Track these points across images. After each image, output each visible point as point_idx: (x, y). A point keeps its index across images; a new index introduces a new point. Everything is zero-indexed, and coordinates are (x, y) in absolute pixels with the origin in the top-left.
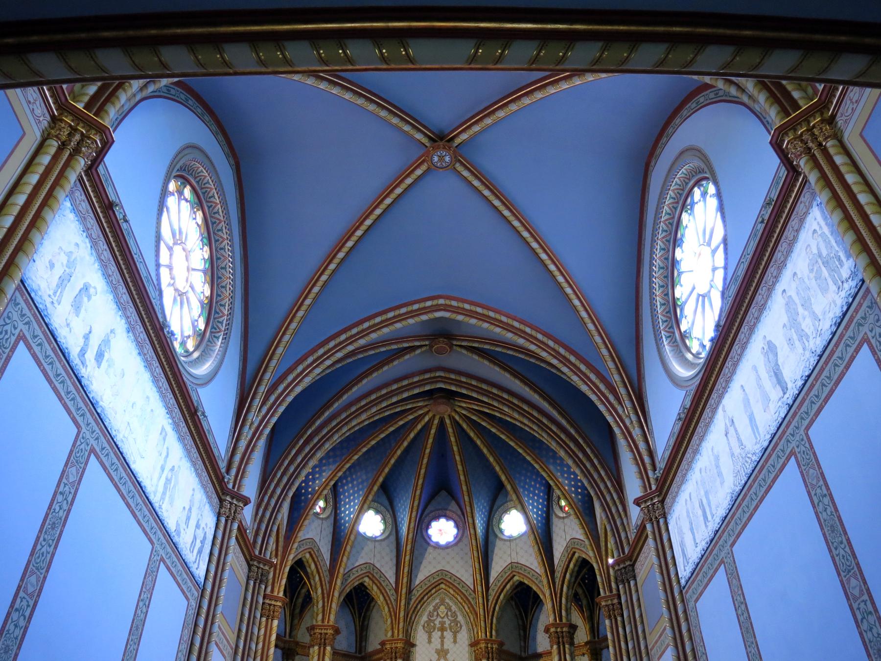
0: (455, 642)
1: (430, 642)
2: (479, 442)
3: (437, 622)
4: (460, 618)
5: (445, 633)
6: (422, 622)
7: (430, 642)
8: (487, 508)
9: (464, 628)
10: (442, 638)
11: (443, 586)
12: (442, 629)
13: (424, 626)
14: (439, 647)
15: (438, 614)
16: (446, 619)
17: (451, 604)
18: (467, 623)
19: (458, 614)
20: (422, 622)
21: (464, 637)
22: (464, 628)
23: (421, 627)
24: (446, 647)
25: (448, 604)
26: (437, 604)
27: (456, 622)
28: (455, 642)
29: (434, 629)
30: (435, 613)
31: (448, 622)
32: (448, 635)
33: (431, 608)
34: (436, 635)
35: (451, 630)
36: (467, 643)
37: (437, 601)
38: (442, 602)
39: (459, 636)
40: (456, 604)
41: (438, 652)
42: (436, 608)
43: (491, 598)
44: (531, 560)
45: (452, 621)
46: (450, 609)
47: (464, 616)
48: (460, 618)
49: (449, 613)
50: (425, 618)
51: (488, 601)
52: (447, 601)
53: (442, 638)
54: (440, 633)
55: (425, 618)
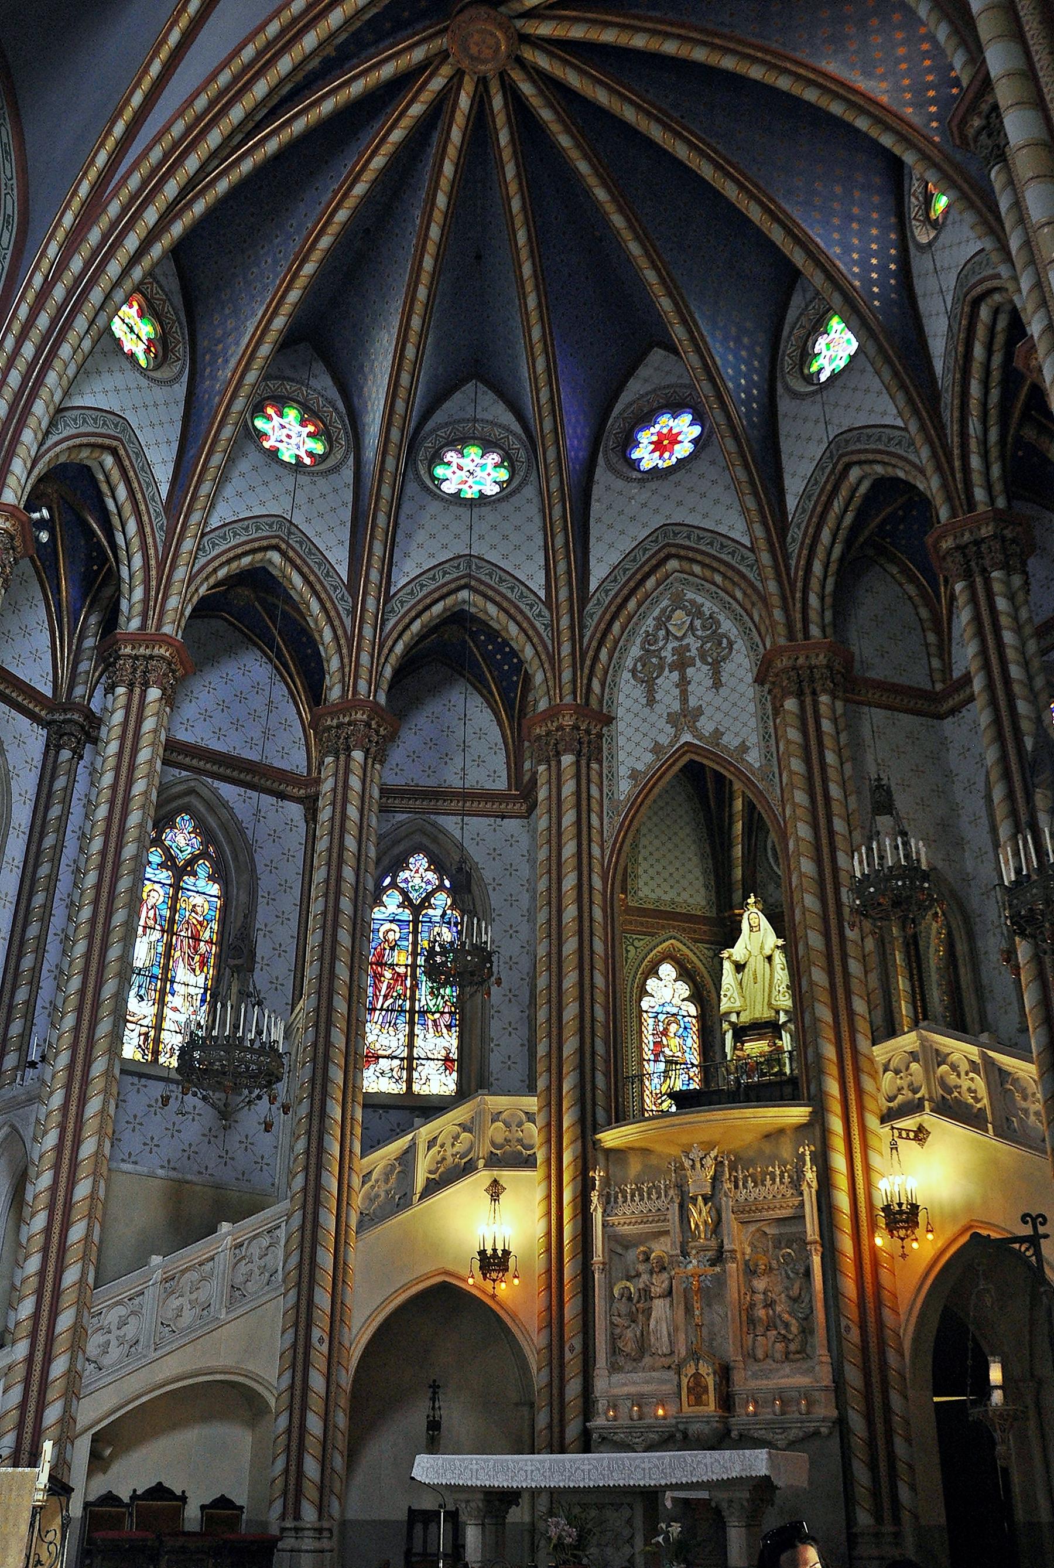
0: (717, 684)
1: (651, 701)
2: (629, 114)
3: (668, 654)
4: (727, 626)
5: (690, 671)
6: (629, 663)
7: (651, 701)
8: (762, 337)
9: (739, 645)
10: (684, 683)
11: (673, 564)
12: (682, 664)
13: (634, 672)
14: (676, 706)
15: (668, 632)
16: (690, 640)
17: (700, 600)
18: (746, 632)
19: (721, 618)
20: (629, 663)
21: (740, 666)
22: (739, 645)
23: (627, 675)
24: (693, 702)
25: (693, 602)
26: (663, 611)
27: (717, 637)
28: (717, 684)
29: (662, 669)
30: (662, 633)
31: (694, 644)
32: (699, 674)
33: (650, 623)
34: (668, 681)
35: (704, 661)
36: (749, 678)
37: (665, 603)
38: (678, 602)
39: (728, 667)
40: (714, 597)
41: (673, 719)
42: (662, 623)
43: (794, 548)
44: (882, 408)
45: (704, 640)
46: (696, 611)
47: (737, 619)
48: (727, 626)
49: (698, 623)
50: (635, 651)
51: (787, 557)
52: (690, 595)
53: (684, 683)
54: (675, 676)
55: (635, 651)
